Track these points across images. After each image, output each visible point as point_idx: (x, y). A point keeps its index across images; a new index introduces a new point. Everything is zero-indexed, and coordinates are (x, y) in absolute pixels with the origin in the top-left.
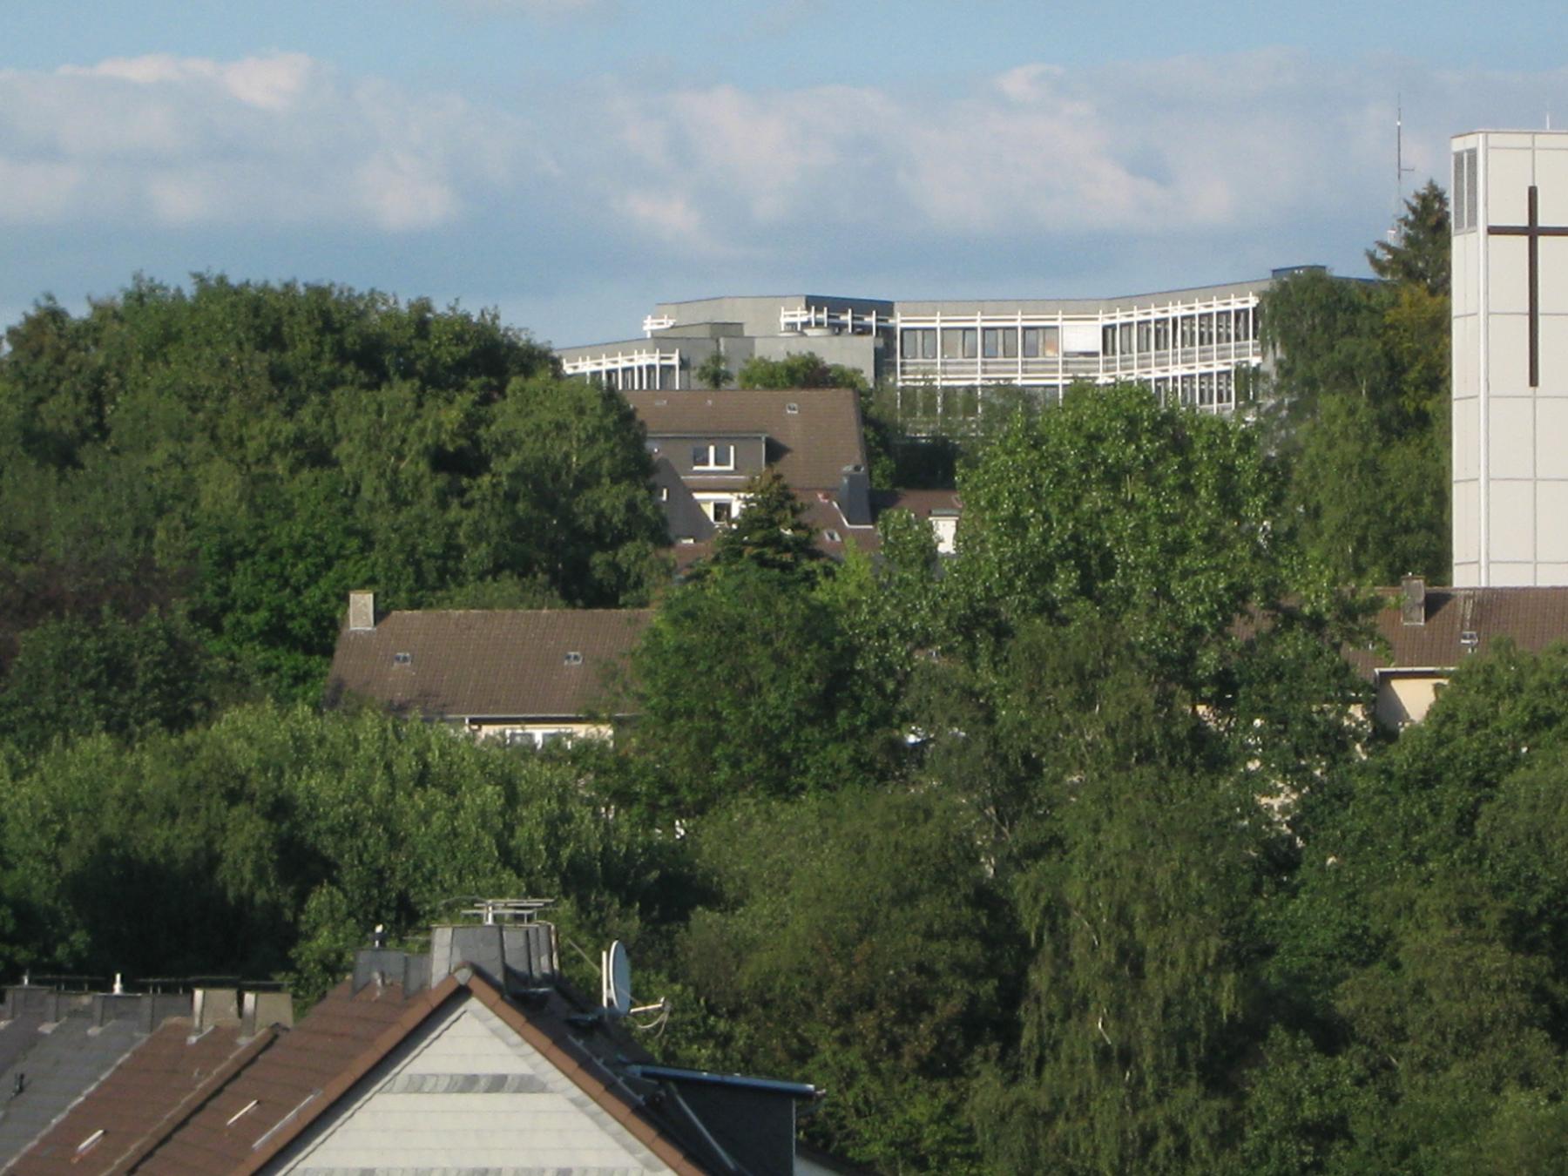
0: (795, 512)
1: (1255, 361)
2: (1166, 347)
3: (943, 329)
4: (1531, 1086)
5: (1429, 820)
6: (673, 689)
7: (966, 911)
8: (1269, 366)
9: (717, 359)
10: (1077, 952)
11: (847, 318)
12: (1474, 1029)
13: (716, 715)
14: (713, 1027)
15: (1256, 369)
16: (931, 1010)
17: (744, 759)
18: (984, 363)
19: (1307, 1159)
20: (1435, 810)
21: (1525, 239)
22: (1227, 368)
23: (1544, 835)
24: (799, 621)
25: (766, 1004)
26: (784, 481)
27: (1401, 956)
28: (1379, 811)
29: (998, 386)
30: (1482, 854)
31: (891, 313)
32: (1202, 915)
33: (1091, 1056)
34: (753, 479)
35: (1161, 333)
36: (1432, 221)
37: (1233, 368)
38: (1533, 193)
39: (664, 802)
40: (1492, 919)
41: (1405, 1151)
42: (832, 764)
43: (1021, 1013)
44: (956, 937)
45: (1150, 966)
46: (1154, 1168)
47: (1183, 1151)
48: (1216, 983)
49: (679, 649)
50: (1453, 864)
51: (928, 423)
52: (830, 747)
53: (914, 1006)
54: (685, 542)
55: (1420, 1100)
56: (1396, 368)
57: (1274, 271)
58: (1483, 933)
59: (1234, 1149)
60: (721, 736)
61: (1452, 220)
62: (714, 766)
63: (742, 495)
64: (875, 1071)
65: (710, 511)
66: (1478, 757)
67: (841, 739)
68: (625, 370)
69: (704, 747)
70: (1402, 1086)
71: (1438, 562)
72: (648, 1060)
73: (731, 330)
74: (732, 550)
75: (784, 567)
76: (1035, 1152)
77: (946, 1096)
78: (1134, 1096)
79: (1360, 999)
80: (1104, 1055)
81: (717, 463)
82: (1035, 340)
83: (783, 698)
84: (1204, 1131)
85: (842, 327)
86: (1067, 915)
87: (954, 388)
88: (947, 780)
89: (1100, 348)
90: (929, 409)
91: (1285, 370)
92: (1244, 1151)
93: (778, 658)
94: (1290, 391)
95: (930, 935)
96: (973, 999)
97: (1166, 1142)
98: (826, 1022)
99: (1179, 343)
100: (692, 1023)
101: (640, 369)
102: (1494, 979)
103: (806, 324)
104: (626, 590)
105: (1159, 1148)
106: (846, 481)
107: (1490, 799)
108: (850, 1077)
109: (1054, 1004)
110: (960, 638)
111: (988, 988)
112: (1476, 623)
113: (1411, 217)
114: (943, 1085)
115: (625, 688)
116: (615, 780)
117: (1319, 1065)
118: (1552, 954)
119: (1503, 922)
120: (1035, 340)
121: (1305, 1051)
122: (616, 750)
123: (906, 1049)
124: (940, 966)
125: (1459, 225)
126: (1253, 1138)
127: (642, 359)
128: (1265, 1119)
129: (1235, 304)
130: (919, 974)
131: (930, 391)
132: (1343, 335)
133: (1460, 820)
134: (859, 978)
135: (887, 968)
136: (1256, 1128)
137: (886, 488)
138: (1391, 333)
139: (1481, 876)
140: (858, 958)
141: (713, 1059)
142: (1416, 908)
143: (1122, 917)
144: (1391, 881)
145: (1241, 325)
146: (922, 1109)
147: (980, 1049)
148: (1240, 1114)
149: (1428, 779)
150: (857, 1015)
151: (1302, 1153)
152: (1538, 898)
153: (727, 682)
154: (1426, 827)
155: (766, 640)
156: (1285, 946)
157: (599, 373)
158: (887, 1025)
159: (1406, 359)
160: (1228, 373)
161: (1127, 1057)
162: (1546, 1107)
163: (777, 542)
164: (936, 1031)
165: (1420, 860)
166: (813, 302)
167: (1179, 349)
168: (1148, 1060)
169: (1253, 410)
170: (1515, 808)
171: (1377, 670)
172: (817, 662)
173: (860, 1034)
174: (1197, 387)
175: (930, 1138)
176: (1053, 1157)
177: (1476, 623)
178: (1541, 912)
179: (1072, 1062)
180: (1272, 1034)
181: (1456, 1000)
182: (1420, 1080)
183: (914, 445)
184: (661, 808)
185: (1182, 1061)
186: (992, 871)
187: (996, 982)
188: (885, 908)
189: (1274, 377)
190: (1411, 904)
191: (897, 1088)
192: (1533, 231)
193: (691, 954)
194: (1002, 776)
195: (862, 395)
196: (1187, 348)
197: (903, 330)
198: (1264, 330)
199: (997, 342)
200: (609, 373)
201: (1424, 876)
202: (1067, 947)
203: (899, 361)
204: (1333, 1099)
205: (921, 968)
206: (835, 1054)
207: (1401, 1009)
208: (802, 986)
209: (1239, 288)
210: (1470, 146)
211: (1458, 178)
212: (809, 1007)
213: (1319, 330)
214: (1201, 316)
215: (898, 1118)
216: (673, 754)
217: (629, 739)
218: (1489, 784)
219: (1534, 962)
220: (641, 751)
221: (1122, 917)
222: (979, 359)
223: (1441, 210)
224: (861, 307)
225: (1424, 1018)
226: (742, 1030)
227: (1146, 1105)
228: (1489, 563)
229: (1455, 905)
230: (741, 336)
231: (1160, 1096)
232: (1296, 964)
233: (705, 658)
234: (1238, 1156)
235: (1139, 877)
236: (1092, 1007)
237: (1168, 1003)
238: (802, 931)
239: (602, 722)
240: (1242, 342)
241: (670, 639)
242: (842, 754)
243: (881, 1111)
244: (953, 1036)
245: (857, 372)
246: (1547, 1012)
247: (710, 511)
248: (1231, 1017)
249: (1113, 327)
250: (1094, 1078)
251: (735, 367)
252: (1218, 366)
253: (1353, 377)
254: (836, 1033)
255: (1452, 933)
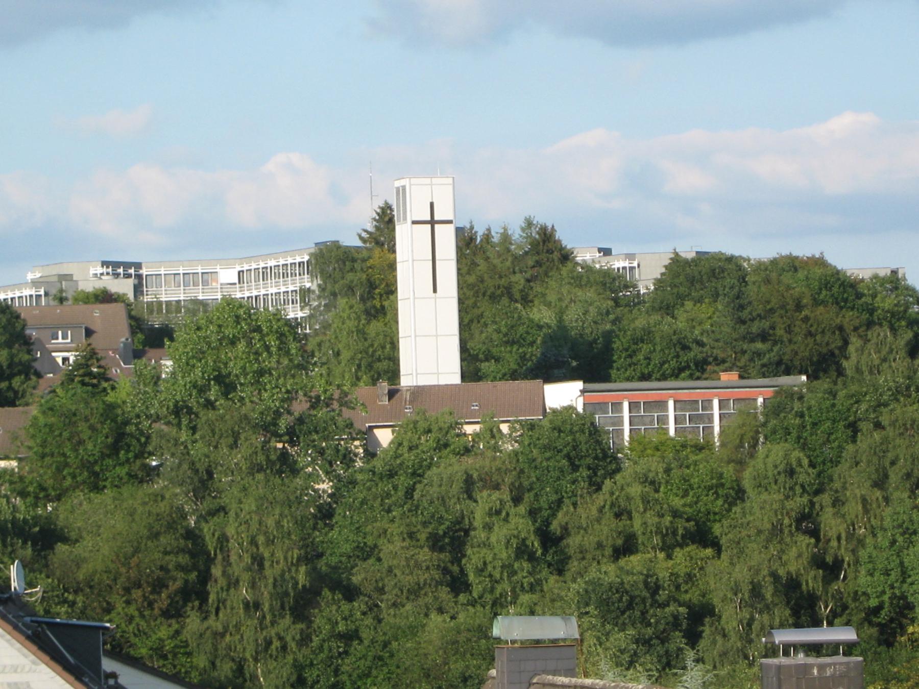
0: (98, 360)
1: (308, 285)
2: (267, 280)
3: (165, 274)
4: (442, 613)
5: (392, 492)
6: (44, 444)
7: (182, 541)
8: (314, 287)
9: (61, 291)
10: (233, 558)
11: (121, 270)
12: (416, 587)
13: (64, 455)
14: (67, 598)
15: (309, 289)
16: (167, 587)
17: (77, 474)
18: (184, 290)
19: (341, 650)
20: (395, 488)
21: (429, 226)
22: (295, 289)
23: (446, 498)
24: (101, 411)
25: (91, 587)
26: (92, 346)
27: (381, 555)
28: (369, 489)
29: (191, 300)
30: (417, 507)
31: (141, 268)
32: (290, 539)
33: (241, 606)
34: (78, 346)
35: (265, 274)
36: (387, 219)
37: (298, 289)
38: (432, 205)
39: (41, 495)
40: (423, 536)
41: (386, 644)
42: (118, 476)
43: (209, 587)
44: (177, 553)
45: (267, 564)
46: (271, 656)
47: (284, 648)
48: (297, 571)
49: (46, 425)
50: (404, 513)
51: (159, 318)
52: (117, 468)
53: (159, 585)
54: (48, 375)
55: (392, 620)
56: (372, 286)
57: (316, 244)
58: (419, 544)
59: (307, 646)
60: (67, 465)
61: (396, 218)
62: (64, 478)
63: (73, 353)
64: (142, 616)
65: (60, 361)
66: (414, 463)
67: (122, 465)
68: (19, 297)
69: (59, 470)
70: (384, 615)
71: (394, 374)
72: (35, 615)
73: (68, 277)
74: (70, 378)
75: (94, 386)
76: (216, 650)
77: (176, 626)
78: (261, 624)
79: (363, 576)
80: (247, 605)
81: (63, 338)
82: (207, 278)
83: (95, 446)
84: (294, 639)
85: (118, 275)
86: (228, 541)
87: (170, 301)
88: (171, 481)
89: (236, 281)
90: (160, 310)
91: (322, 289)
92: (312, 647)
93: (92, 428)
94: (325, 298)
95: (166, 553)
96: (186, 581)
97: (276, 644)
98: (119, 594)
99: (273, 278)
100: (57, 596)
101: (26, 297)
102: (424, 564)
103: (102, 274)
104: (19, 399)
105: (273, 647)
106: (122, 345)
107: (420, 482)
108: (131, 619)
109: (222, 582)
110: (173, 417)
111: (193, 576)
112: (411, 402)
113: (377, 218)
114: (173, 621)
115: (22, 444)
116: (18, 486)
117: (345, 607)
118: (450, 552)
119: (428, 538)
120: (207, 278)
121: (339, 600)
122: (19, 473)
123: (156, 605)
124: (170, 567)
125: (399, 220)
126: (316, 641)
127: (27, 292)
128: (321, 632)
129: (298, 259)
130: (161, 571)
131: (160, 303)
132: (348, 272)
133: (406, 492)
134: (133, 574)
135: (146, 569)
136: (317, 636)
137: (141, 347)
138: (370, 270)
139: (417, 517)
140: (132, 565)
141: (67, 612)
142: (388, 533)
143: (253, 542)
144: (376, 521)
145: (301, 269)
146: (164, 632)
147: (190, 605)
148: (309, 630)
149: (392, 474)
150: (133, 591)
151: (339, 647)
152: (443, 527)
153: (69, 440)
154: (391, 496)
155: (87, 419)
156: (329, 552)
157: (7, 299)
158: (147, 595)
159: (377, 282)
160: (296, 291)
161: (257, 606)
162: (450, 621)
163: (90, 374)
164: (169, 597)
165: (389, 511)
166: (105, 264)
167: (273, 281)
168: (266, 607)
169: (308, 308)
170: (432, 485)
171: (367, 425)
172: (109, 429)
173: (135, 599)
174: (282, 297)
175: (169, 645)
176: (224, 652)
177: (411, 402)
178: (445, 533)
179: (232, 609)
180: (323, 593)
181: (408, 575)
182: (392, 611)
183: (152, 329)
184: (40, 498)
185: (283, 607)
186: (193, 522)
187: (196, 573)
188: (144, 541)
189: (317, 292)
190: (385, 531)
191: (153, 624)
192: (432, 222)
193: (56, 565)
194: (196, 479)
195: (129, 305)
196: (277, 280)
197: (146, 275)
198: (312, 270)
199: (189, 279)
200: (12, 299)
201: (391, 518)
202: (228, 556)
203: (145, 289)
204: (352, 622)
205: (162, 568)
206: (123, 608)
207: (382, 579)
208: (108, 577)
209: (300, 251)
210: (402, 184)
211: (398, 199)
212: (111, 588)
213: (337, 270)
214: (283, 265)
215: (154, 637)
216: (45, 473)
217: (24, 467)
218: (419, 475)
219: (442, 556)
220: (29, 473)
221: (253, 542)
222: (182, 288)
223: (391, 214)
224: (127, 265)
225: (393, 583)
226: (80, 599)
227: (267, 627)
228: (417, 374)
229: (405, 531)
230: (72, 280)
231: (273, 623)
232: (334, 560)
233: (58, 429)
234: (309, 649)
235: (260, 524)
236: (241, 584)
237: (275, 580)
238: (106, 553)
239: (12, 459)
240: (302, 277)
241: (42, 420)
242: (122, 471)
243: (145, 634)
244: (177, 599)
245: (124, 295)
246: (449, 578)
247: (60, 361)
248: (304, 586)
249: (243, 271)
250: (242, 616)
251: (70, 294)
252: (291, 288)
253: (353, 291)
254: (124, 599)
255: (404, 544)
